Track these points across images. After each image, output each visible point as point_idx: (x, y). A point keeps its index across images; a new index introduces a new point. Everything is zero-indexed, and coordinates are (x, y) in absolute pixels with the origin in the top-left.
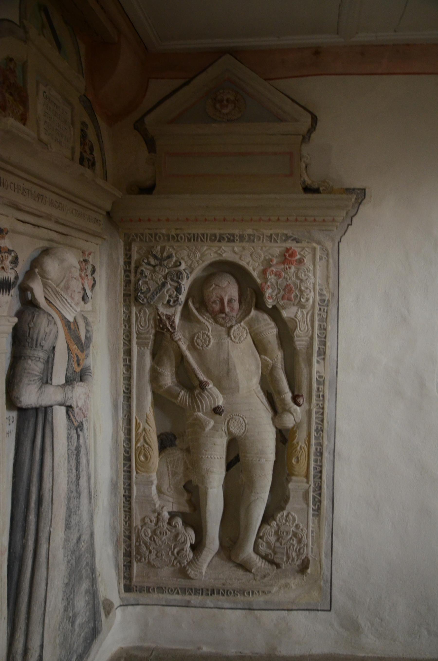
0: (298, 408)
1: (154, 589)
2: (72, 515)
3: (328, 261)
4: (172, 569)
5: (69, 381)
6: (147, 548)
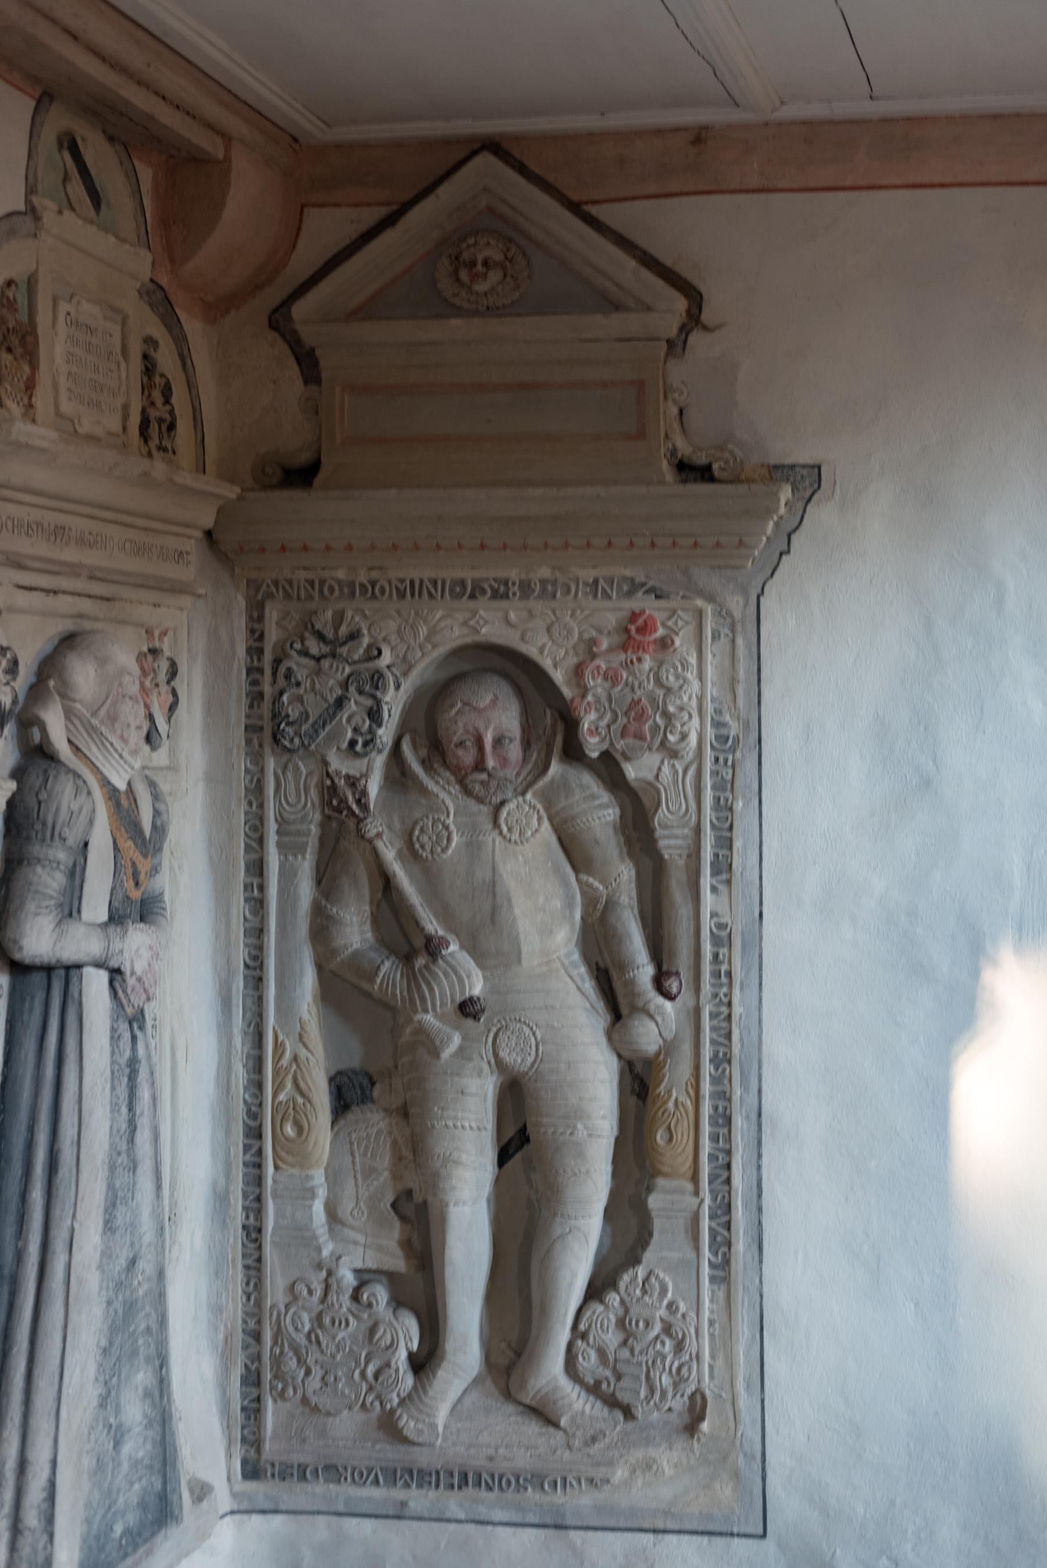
0: (668, 1005)
1: (317, 1470)
2: (118, 1202)
3: (733, 641)
4: (359, 1417)
6: (299, 1361)
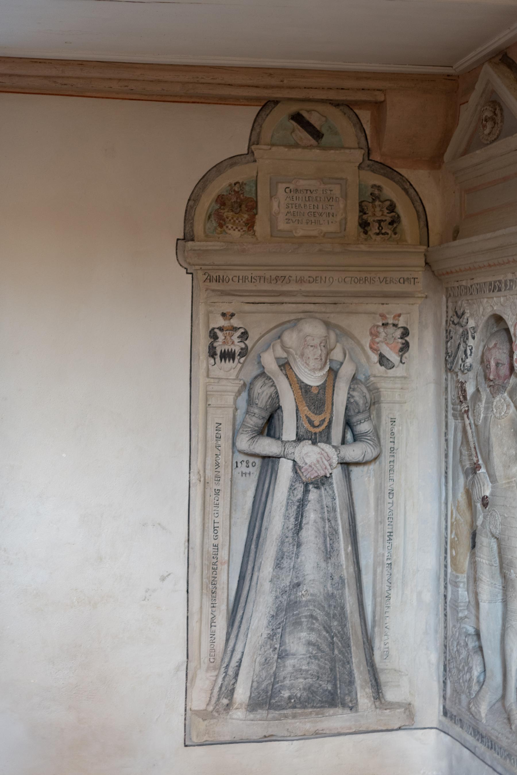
2: (285, 557)
5: (299, 439)
